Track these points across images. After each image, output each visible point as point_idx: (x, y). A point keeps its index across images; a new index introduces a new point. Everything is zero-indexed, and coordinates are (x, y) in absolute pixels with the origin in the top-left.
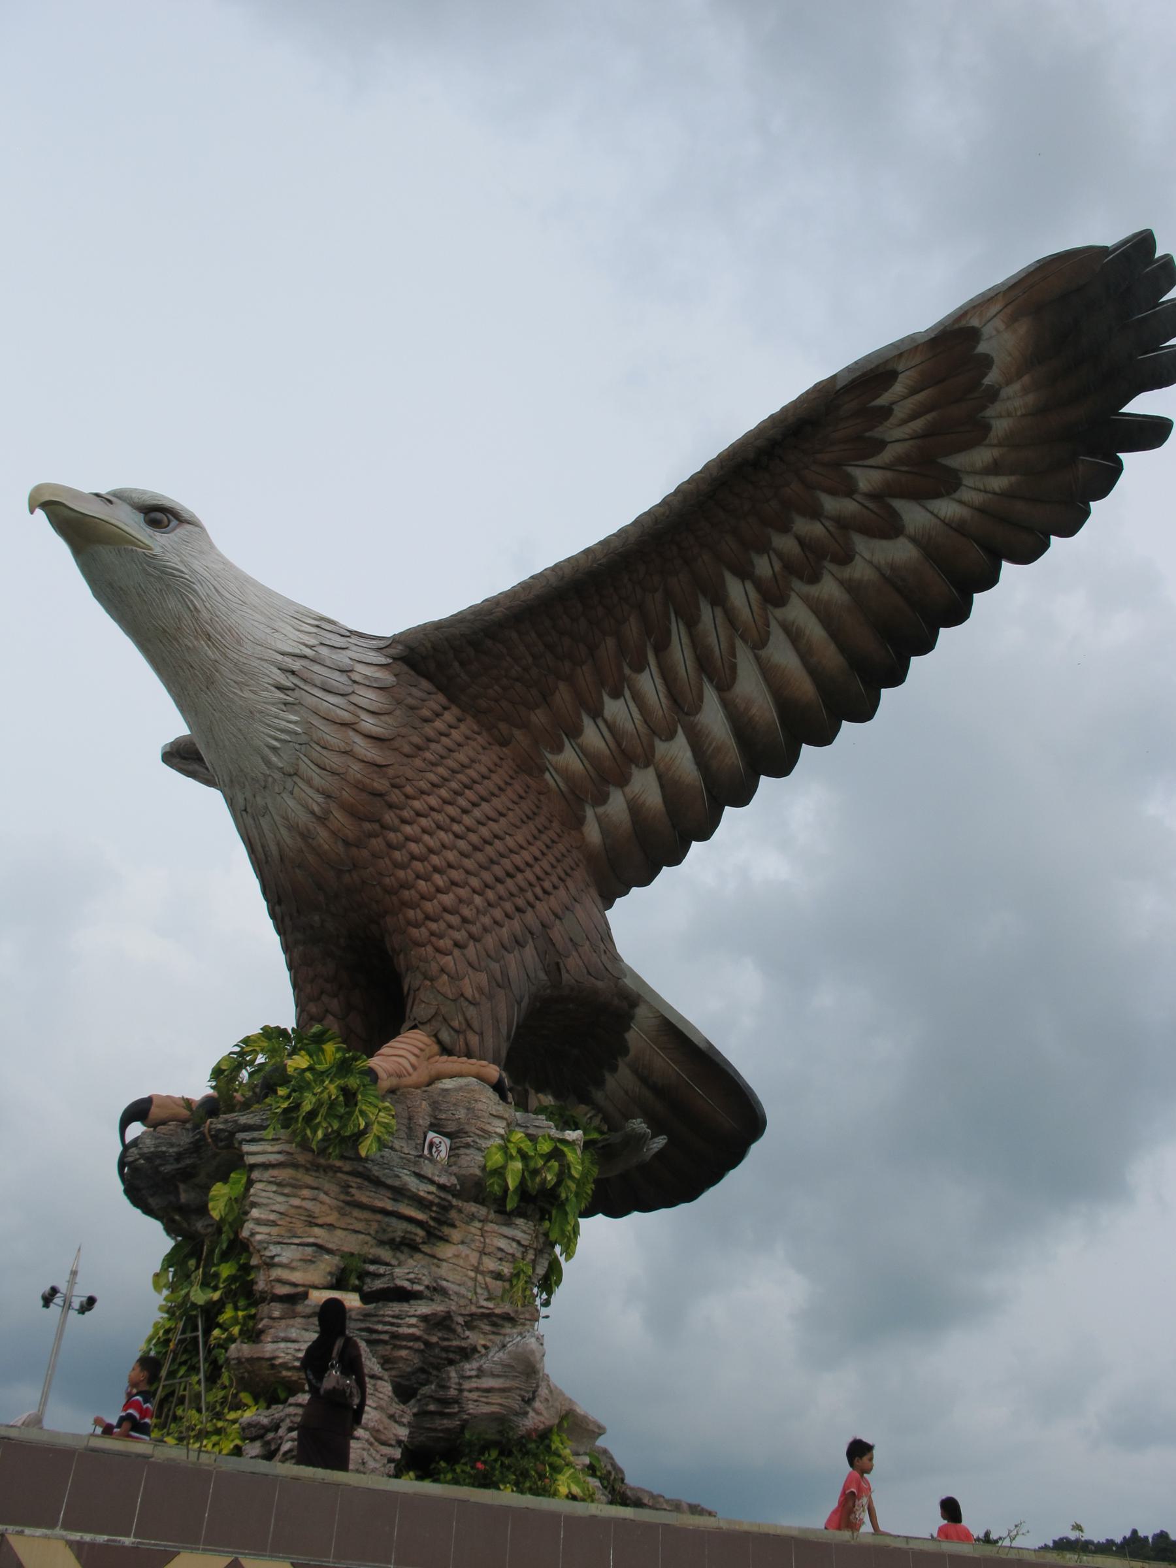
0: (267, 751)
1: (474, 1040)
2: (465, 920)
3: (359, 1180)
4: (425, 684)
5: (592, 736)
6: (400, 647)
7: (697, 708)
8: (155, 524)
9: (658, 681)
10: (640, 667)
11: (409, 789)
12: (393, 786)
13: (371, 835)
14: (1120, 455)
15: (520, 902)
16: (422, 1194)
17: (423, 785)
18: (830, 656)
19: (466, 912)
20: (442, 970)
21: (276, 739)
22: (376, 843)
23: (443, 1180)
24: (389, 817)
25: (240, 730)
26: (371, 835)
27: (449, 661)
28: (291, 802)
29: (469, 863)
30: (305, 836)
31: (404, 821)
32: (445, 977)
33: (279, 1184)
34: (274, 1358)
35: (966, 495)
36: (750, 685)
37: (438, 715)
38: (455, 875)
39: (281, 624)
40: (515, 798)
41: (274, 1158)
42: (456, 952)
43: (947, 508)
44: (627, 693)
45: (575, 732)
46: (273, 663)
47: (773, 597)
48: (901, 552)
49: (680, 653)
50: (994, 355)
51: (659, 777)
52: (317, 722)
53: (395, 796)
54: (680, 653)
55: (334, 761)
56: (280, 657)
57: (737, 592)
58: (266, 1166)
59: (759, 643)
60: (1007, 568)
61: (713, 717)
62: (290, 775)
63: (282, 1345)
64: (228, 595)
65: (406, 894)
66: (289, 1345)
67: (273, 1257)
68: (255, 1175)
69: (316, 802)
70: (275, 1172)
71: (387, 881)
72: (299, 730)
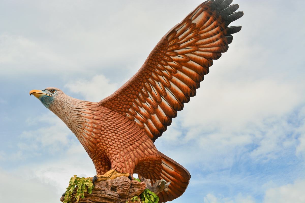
1: (124, 169)
2: (119, 148)
3: (97, 197)
4: (106, 108)
6: (100, 103)
8: (53, 92)
11: (105, 127)
12: (102, 127)
13: (99, 136)
14: (231, 35)
15: (131, 143)
16: (111, 198)
17: (108, 125)
19: (119, 146)
20: (116, 158)
22: (101, 138)
23: (114, 195)
24: (102, 133)
26: (99, 136)
27: (112, 104)
29: (119, 138)
31: (105, 133)
32: (117, 159)
37: (109, 113)
38: (116, 140)
39: (77, 104)
40: (128, 125)
42: (118, 154)
44: (146, 102)
50: (196, 23)
53: (103, 129)
60: (214, 61)
64: (66, 101)
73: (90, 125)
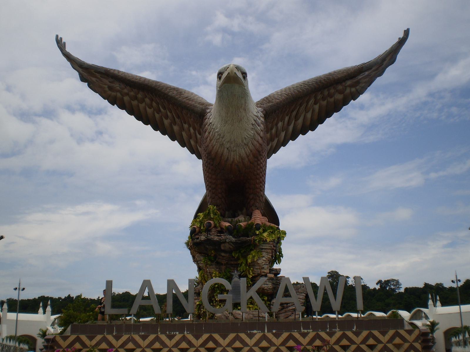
0: (244, 138)
5: (274, 131)
7: (290, 125)
9: (288, 118)
10: (287, 115)
18: (316, 117)
21: (247, 136)
24: (259, 158)
25: (241, 133)
28: (243, 151)
30: (242, 159)
33: (267, 253)
34: (264, 288)
35: (358, 87)
36: (300, 121)
41: (268, 247)
43: (353, 89)
45: (272, 129)
46: (253, 118)
47: (315, 103)
48: (339, 97)
49: (294, 113)
51: (278, 140)
52: (256, 134)
53: (261, 153)
54: (294, 113)
55: (255, 143)
56: (254, 117)
57: (312, 101)
58: (265, 249)
59: (307, 112)
61: (291, 128)
62: (246, 145)
63: (265, 285)
65: (258, 176)
66: (267, 285)
67: (264, 267)
68: (263, 250)
69: (248, 151)
70: (268, 250)
71: (255, 172)
72: (252, 135)
73: (255, 143)
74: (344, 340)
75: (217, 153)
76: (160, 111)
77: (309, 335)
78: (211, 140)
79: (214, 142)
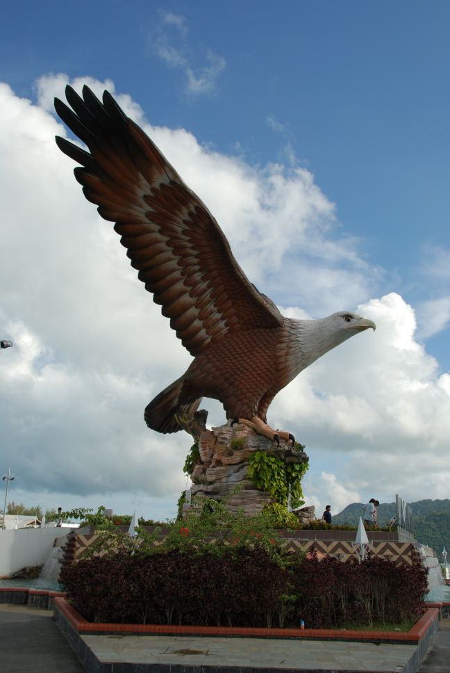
74: (340, 549)
75: (285, 367)
76: (190, 275)
77: (380, 545)
78: (287, 354)
79: (290, 358)
